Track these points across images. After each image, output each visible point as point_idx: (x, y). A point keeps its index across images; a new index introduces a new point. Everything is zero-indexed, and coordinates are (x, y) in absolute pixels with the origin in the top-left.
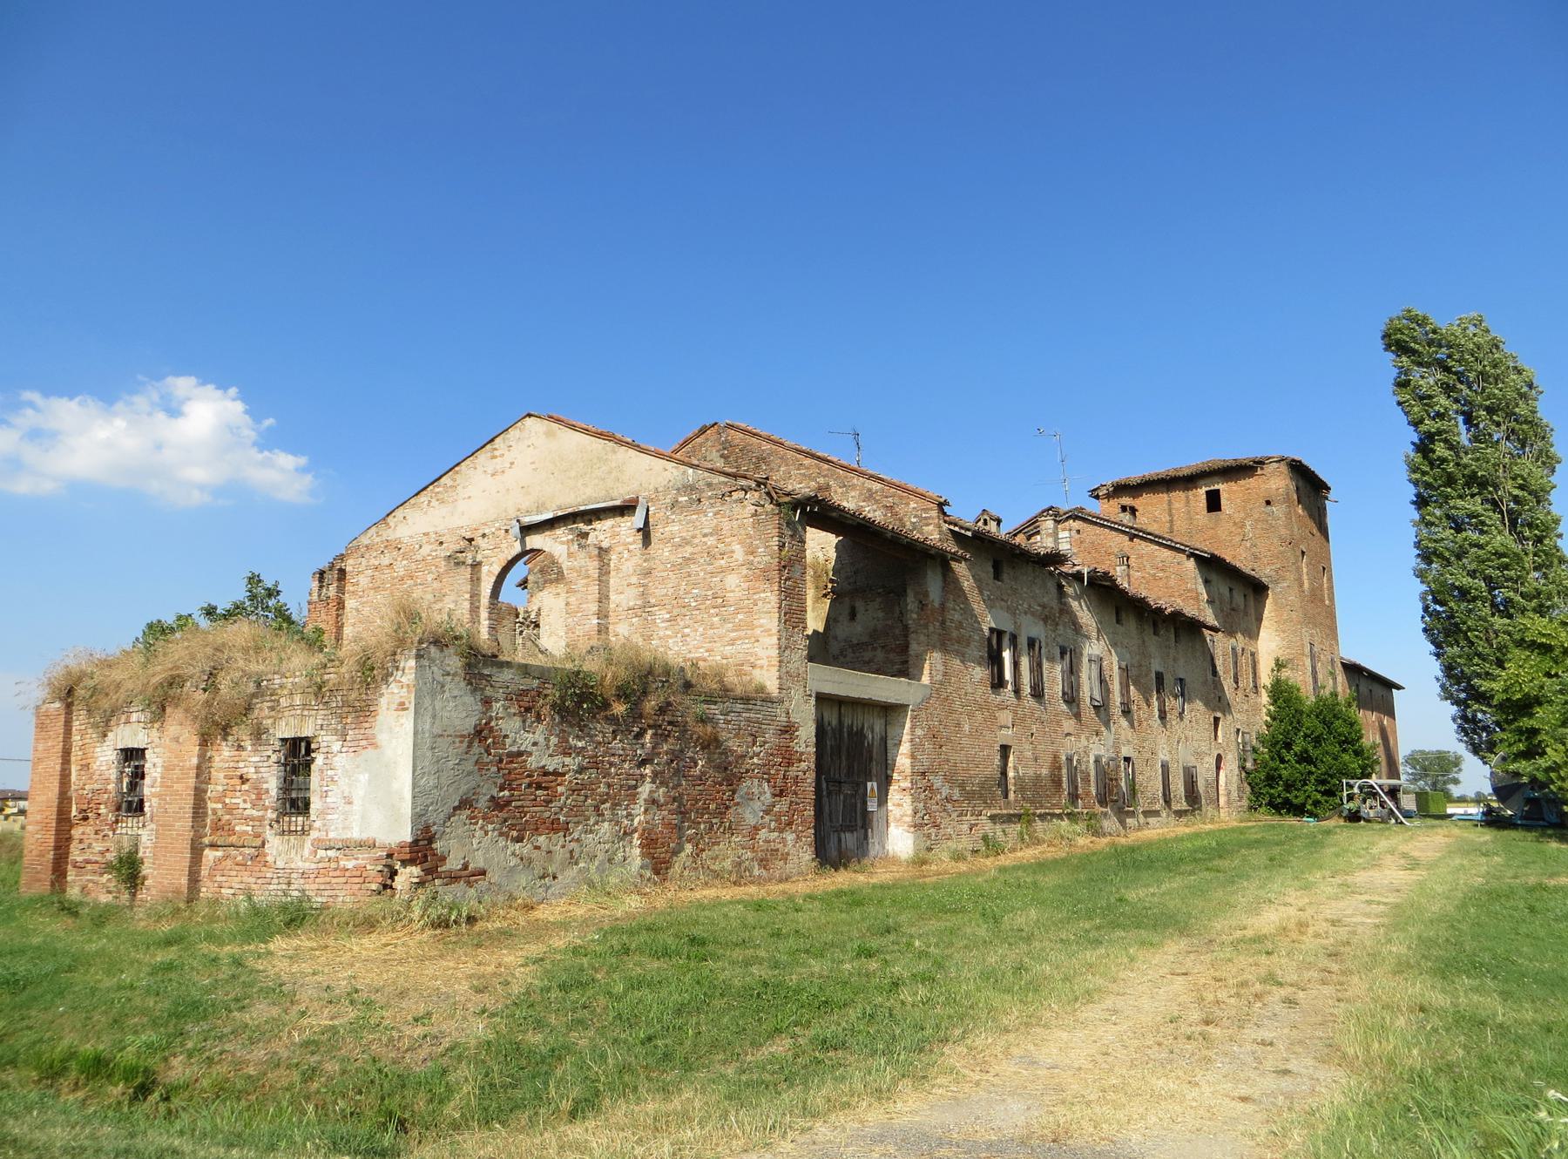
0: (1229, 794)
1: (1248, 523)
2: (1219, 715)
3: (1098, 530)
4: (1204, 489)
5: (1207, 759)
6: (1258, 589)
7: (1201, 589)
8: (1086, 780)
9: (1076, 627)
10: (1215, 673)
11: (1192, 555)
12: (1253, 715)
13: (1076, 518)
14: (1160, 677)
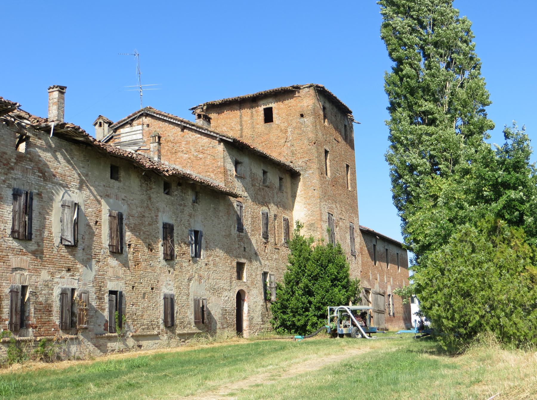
0: (251, 319)
1: (289, 130)
2: (243, 260)
3: (161, 124)
4: (263, 107)
5: (226, 293)
6: (294, 175)
7: (230, 166)
8: (48, 309)
9: (45, 174)
10: (241, 229)
11: (221, 141)
12: (274, 264)
13: (147, 115)
14: (168, 230)
